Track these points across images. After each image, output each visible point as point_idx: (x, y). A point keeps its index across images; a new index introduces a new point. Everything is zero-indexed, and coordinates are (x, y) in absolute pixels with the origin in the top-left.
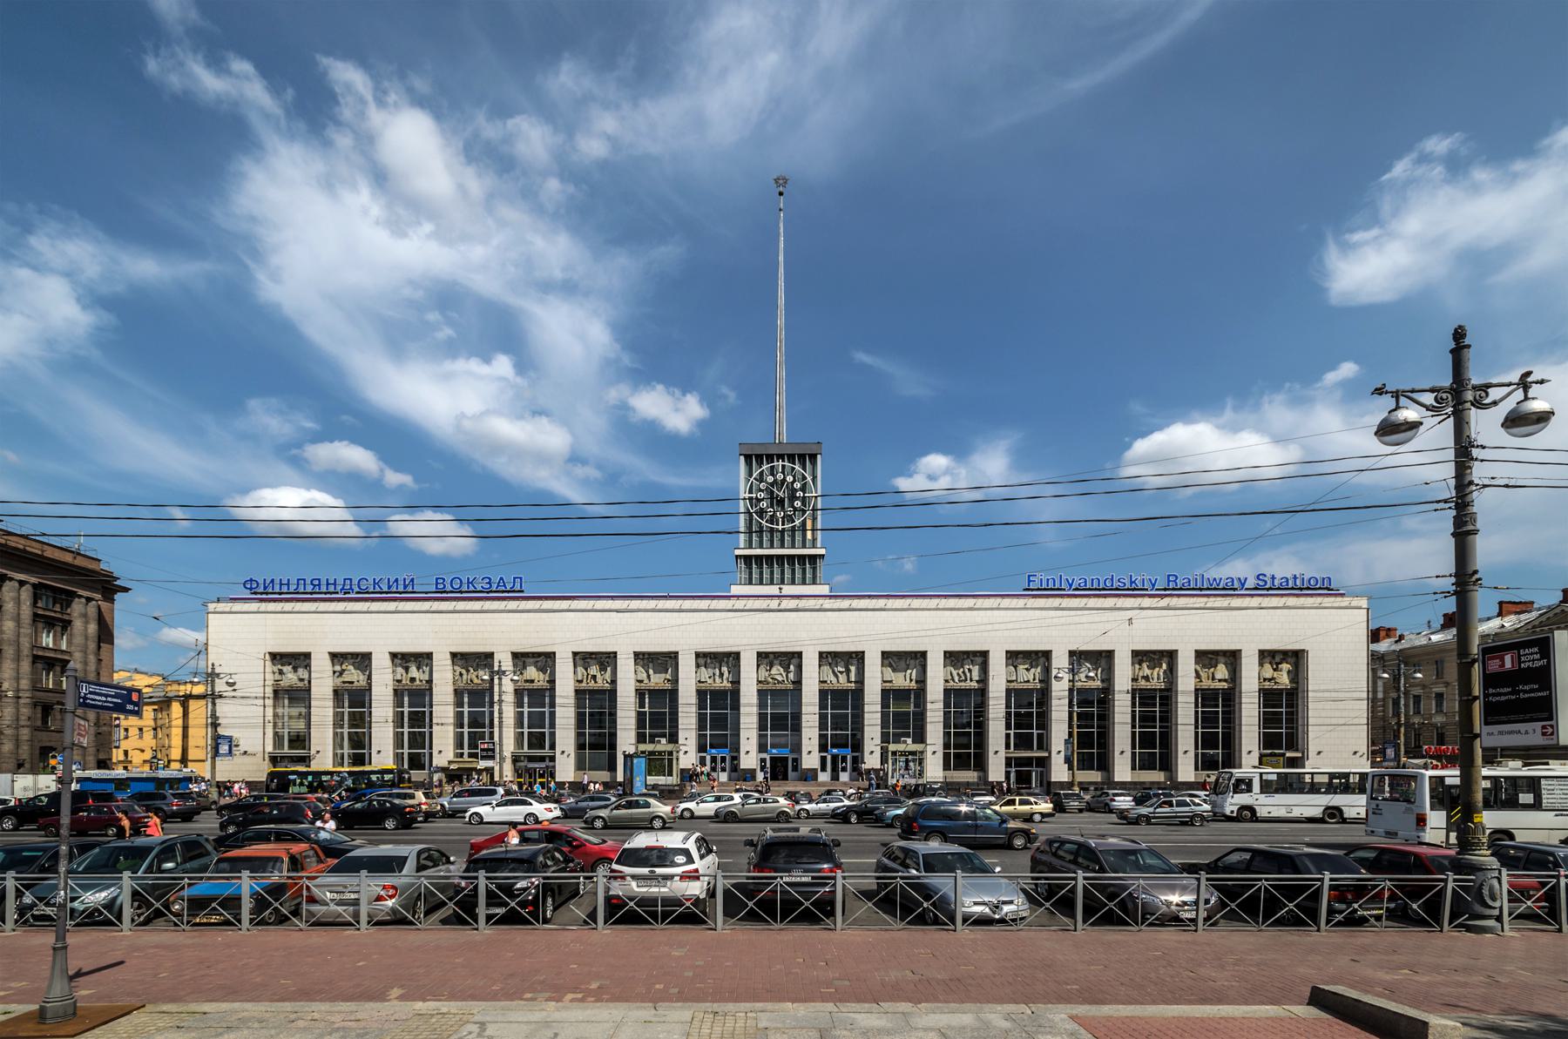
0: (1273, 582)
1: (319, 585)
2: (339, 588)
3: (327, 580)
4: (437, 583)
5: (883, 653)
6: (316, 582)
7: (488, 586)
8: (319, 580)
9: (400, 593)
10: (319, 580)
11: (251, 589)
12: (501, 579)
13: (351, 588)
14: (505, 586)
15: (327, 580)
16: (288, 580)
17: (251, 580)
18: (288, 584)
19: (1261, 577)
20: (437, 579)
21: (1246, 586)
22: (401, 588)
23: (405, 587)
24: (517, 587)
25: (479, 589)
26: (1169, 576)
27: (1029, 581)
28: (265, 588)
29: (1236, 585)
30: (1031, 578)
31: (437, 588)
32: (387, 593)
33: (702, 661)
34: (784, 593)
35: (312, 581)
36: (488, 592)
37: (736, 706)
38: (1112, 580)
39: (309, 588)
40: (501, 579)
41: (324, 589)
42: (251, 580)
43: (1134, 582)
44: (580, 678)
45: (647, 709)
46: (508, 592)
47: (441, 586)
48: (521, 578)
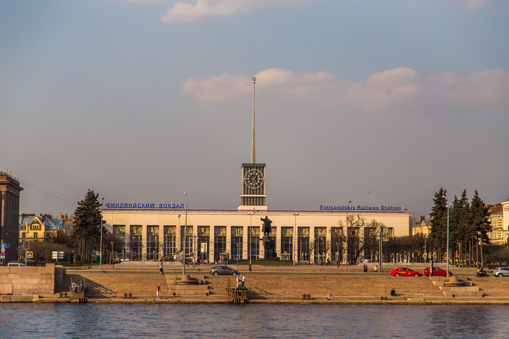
0: (385, 208)
1: (127, 205)
2: (132, 207)
3: (129, 204)
4: (160, 205)
5: (282, 227)
6: (126, 205)
7: (174, 206)
8: (127, 204)
9: (149, 208)
10: (127, 204)
11: (108, 206)
12: (178, 204)
13: (136, 206)
14: (179, 206)
15: (129, 204)
16: (131, 204)
17: (108, 204)
18: (118, 205)
19: (382, 207)
20: (160, 204)
21: (378, 209)
22: (150, 207)
23: (151, 206)
24: (182, 207)
25: (172, 207)
26: (358, 206)
27: (321, 207)
28: (112, 206)
29: (376, 209)
30: (322, 206)
31: (160, 207)
32: (146, 208)
33: (233, 228)
34: (255, 209)
35: (125, 204)
36: (174, 208)
37: (242, 241)
38: (343, 207)
39: (124, 206)
40: (178, 204)
41: (128, 206)
42: (108, 204)
43: (349, 208)
44: (199, 233)
45: (217, 242)
46: (179, 208)
47: (161, 206)
48: (183, 204)
